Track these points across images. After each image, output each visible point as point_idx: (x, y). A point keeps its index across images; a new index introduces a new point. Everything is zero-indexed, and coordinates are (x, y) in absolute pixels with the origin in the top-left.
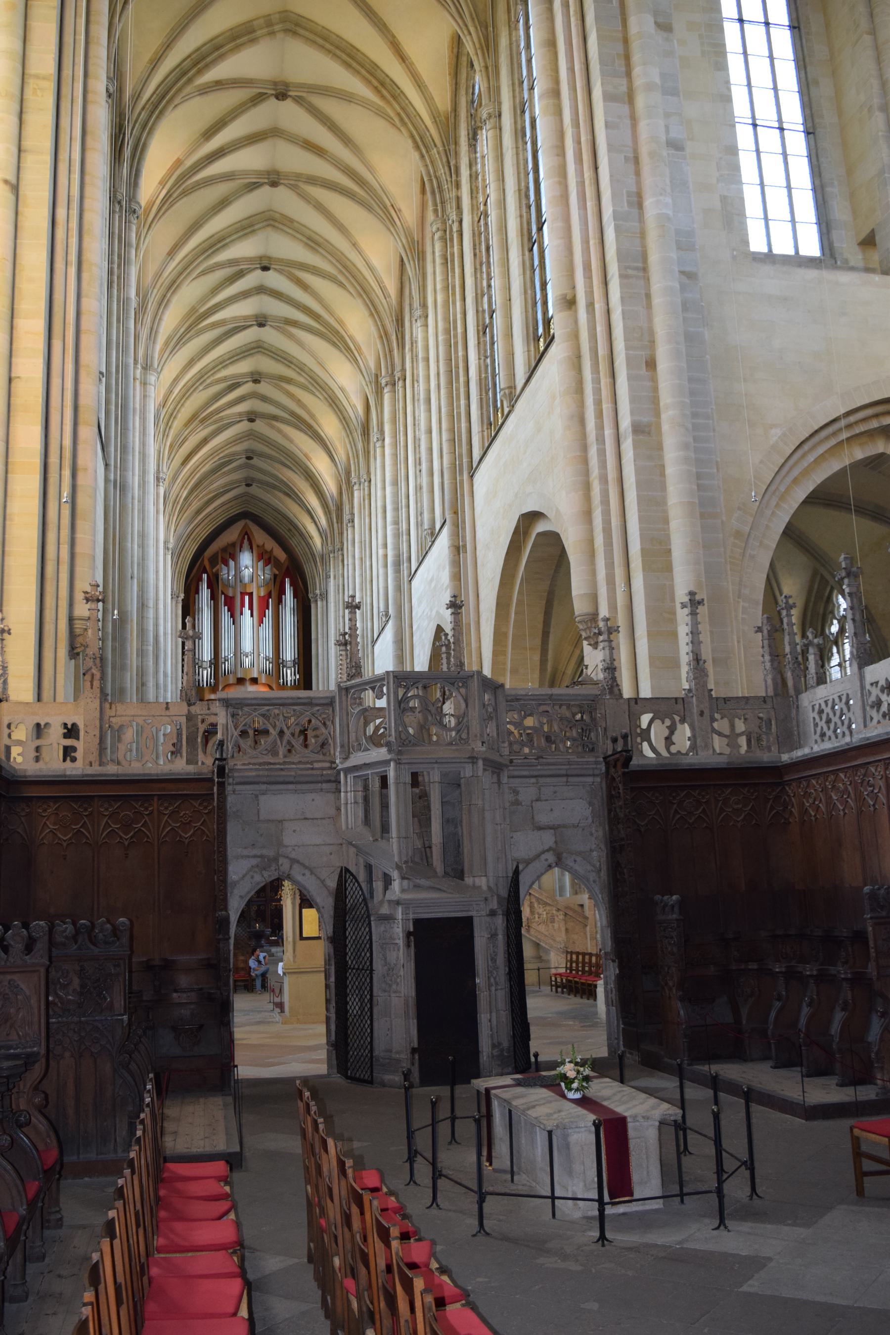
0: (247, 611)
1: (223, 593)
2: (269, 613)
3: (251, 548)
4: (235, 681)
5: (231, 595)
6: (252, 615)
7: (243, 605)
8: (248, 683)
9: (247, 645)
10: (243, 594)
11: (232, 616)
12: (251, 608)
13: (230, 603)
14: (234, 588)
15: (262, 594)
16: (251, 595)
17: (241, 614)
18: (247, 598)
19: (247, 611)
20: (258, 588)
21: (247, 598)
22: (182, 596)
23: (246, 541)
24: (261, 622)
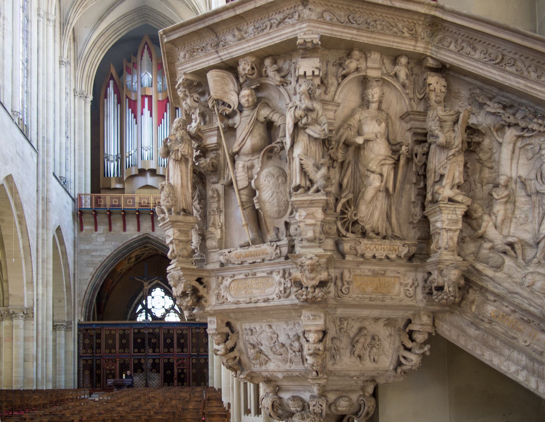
0: (146, 111)
1: (127, 97)
2: (167, 115)
3: (151, 57)
4: (137, 173)
5: (133, 98)
6: (151, 116)
7: (143, 106)
8: (148, 175)
9: (147, 141)
10: (143, 97)
11: (135, 117)
12: (150, 109)
13: (133, 105)
14: (136, 92)
15: (160, 99)
16: (150, 97)
17: (142, 114)
18: (146, 100)
19: (146, 111)
20: (158, 92)
21: (146, 100)
22: (90, 98)
23: (146, 50)
24: (160, 123)
